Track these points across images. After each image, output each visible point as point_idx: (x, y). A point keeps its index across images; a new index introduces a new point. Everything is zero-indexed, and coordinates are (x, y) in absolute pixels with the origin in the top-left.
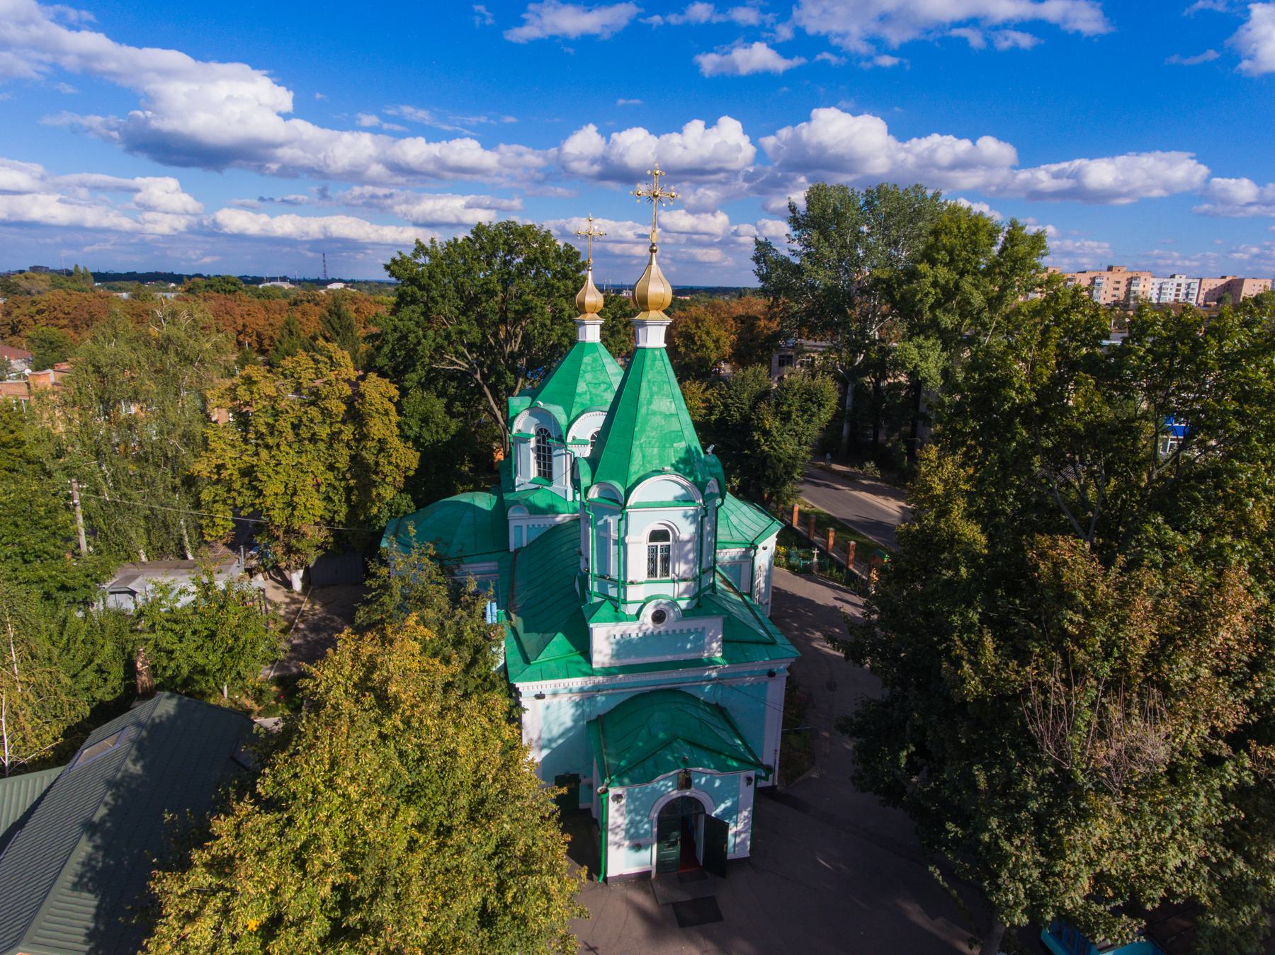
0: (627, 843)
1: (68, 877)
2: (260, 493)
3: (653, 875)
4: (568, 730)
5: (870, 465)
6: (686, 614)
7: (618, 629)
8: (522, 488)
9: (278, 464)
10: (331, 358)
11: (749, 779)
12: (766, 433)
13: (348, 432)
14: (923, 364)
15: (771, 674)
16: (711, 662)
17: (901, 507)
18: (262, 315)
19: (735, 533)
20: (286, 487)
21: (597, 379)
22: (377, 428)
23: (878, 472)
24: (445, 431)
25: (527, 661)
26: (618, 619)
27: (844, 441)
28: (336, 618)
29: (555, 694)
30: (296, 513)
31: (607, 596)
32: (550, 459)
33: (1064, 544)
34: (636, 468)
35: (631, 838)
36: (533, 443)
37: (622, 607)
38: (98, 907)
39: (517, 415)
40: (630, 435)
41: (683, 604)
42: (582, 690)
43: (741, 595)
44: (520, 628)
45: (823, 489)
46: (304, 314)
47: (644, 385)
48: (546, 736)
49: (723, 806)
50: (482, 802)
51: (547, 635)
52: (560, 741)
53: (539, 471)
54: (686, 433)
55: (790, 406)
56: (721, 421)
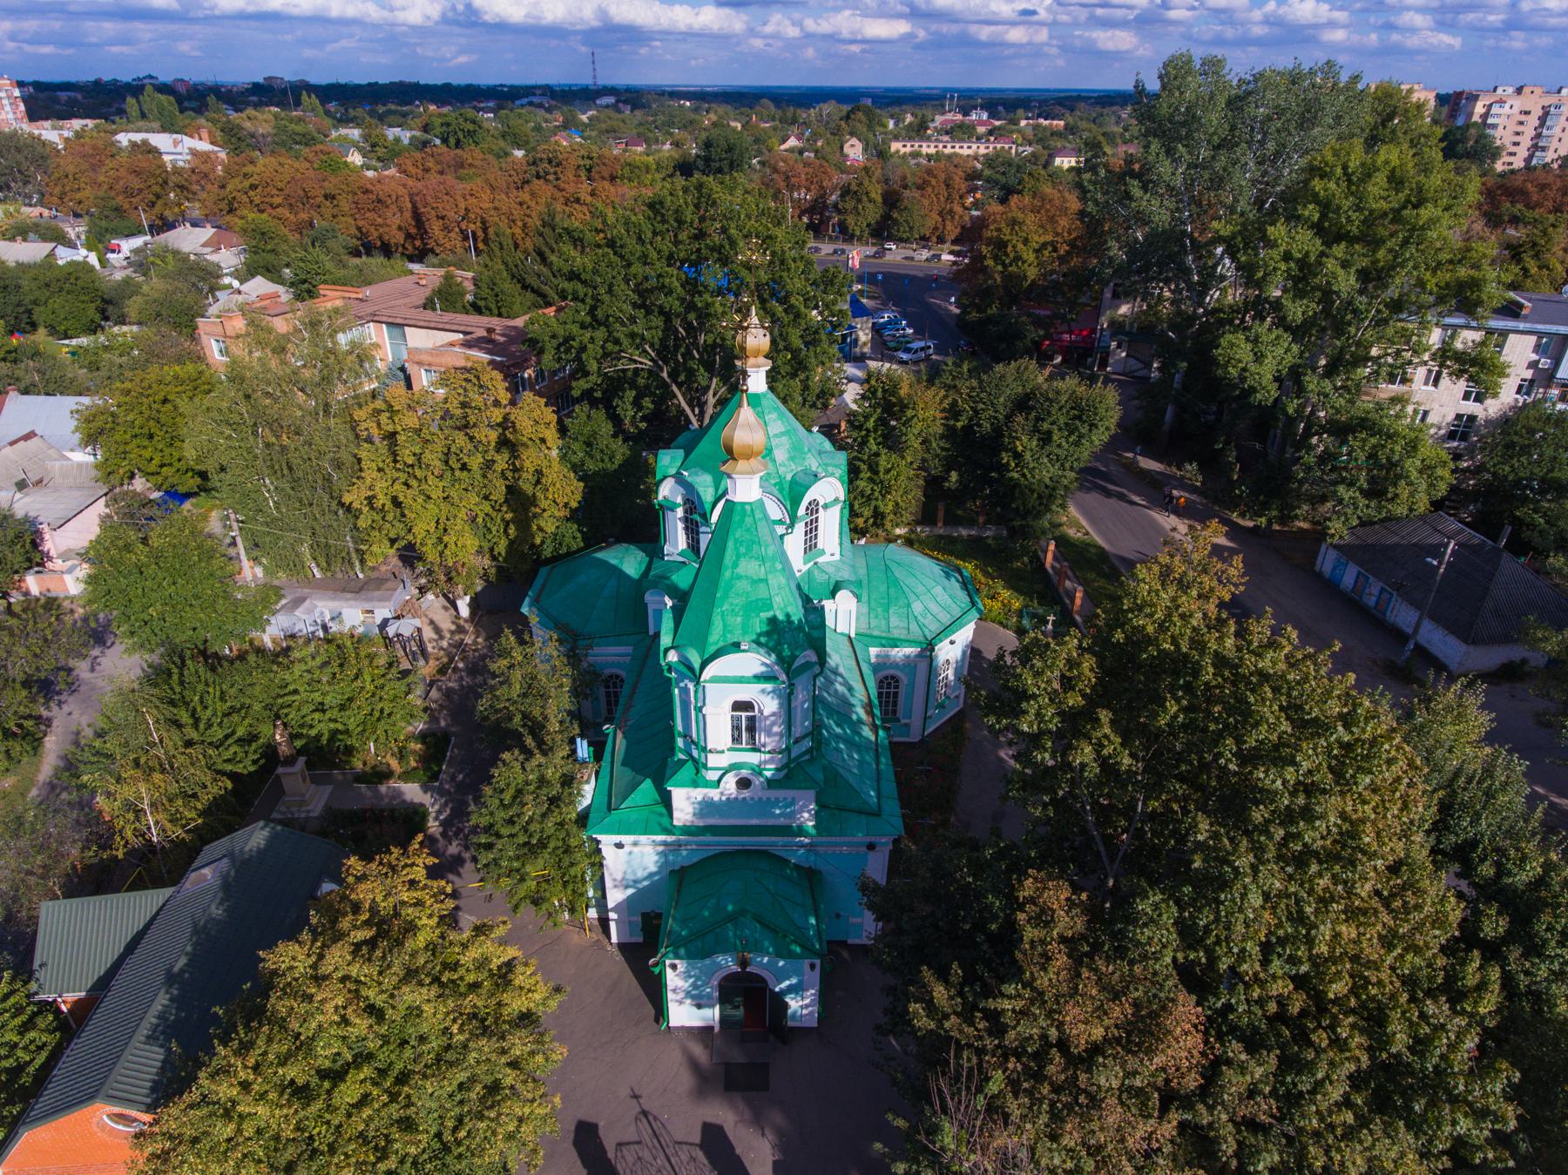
0: (688, 1001)
1: (144, 1031)
2: (410, 530)
3: (717, 1030)
4: (651, 875)
5: (1191, 468)
6: (771, 783)
7: (699, 794)
9: (429, 498)
10: (478, 378)
11: (813, 967)
12: (1018, 456)
13: (501, 461)
14: (1252, 367)
15: (871, 847)
16: (801, 831)
18: (486, 195)
19: (913, 626)
20: (437, 522)
22: (530, 460)
23: (1200, 478)
24: (611, 459)
25: (609, 809)
26: (695, 784)
27: (1166, 428)
29: (635, 844)
30: (447, 552)
31: (690, 755)
32: (698, 533)
33: (1057, 895)
34: (715, 639)
35: (693, 997)
36: (680, 512)
37: (703, 771)
38: (163, 1062)
40: (711, 600)
41: (768, 774)
42: (665, 844)
43: (875, 728)
45: (1113, 501)
46: (533, 194)
47: (730, 544)
48: (630, 877)
49: (787, 983)
50: (448, 1048)
51: (639, 777)
52: (646, 883)
54: (777, 600)
55: (1053, 423)
56: (968, 429)
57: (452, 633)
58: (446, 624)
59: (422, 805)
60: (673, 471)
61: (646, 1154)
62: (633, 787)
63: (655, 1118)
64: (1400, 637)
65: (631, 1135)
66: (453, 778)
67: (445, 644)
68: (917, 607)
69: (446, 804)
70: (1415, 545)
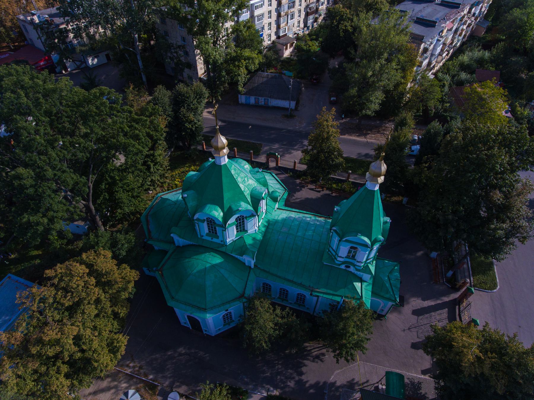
8: (232, 241)
12: (191, 122)
28: (154, 357)
39: (226, 218)
44: (331, 292)
53: (237, 232)
57: (113, 380)
58: (105, 384)
60: (222, 214)
61: (421, 331)
63: (411, 326)
64: (285, 109)
65: (415, 334)
68: (272, 185)
69: (264, 387)
70: (262, 83)
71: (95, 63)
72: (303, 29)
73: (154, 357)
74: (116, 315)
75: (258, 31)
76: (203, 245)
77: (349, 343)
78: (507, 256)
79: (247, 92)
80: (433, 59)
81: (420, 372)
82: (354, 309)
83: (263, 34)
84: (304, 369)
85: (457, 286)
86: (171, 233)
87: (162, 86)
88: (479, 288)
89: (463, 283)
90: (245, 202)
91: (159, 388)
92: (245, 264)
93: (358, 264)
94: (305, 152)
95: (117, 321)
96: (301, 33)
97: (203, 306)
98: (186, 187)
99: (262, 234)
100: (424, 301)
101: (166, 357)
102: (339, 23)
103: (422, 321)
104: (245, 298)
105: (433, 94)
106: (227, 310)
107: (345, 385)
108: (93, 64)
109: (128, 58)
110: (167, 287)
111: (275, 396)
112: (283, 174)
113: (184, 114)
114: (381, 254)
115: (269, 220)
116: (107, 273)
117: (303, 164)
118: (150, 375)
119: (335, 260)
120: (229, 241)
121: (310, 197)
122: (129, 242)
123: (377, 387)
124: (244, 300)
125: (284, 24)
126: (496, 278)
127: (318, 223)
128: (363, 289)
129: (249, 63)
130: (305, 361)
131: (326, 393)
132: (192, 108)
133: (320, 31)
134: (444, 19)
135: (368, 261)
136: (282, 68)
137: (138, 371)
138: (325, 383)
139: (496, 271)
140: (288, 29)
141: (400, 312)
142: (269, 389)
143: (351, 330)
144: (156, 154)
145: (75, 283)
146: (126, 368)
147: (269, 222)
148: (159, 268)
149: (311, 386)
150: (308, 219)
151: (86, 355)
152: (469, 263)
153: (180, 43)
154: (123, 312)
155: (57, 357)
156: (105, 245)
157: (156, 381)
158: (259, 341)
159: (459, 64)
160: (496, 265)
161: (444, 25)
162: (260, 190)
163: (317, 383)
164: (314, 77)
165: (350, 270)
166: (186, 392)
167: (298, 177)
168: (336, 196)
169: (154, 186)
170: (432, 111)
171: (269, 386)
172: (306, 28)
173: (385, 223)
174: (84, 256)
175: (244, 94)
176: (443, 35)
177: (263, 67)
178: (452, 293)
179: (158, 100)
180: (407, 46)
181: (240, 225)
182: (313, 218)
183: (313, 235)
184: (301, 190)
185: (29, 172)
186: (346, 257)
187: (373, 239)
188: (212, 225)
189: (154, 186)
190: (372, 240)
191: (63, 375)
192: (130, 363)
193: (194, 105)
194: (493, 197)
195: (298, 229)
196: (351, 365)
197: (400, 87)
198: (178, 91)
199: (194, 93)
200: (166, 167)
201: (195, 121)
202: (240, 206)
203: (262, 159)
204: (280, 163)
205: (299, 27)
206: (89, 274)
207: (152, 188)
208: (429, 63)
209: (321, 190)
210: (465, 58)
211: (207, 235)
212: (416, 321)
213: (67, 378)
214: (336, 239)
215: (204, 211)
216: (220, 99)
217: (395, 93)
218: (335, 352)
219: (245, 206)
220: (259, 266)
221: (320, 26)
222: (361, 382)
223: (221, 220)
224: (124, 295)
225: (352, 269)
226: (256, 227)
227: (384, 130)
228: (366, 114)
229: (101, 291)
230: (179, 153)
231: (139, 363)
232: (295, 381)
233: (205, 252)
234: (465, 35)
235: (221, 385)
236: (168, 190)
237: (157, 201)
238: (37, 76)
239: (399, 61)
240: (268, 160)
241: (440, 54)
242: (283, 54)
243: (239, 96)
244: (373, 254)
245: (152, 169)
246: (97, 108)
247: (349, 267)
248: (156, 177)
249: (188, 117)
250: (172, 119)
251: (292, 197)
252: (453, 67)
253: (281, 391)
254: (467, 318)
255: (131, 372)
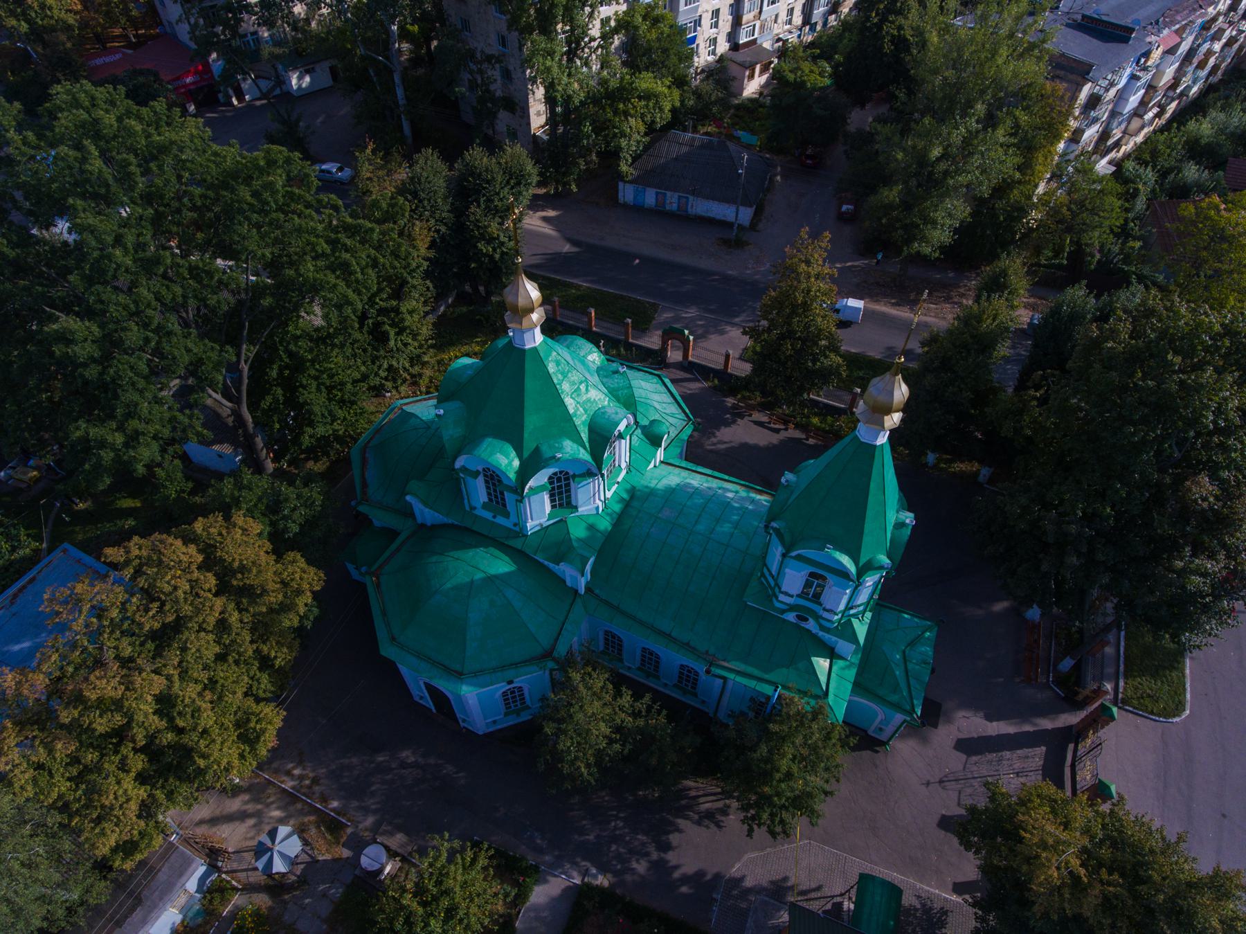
12: (491, 240)
17: (545, 219)
21: (573, 383)
28: (346, 761)
39: (526, 472)
44: (756, 672)
53: (553, 507)
55: (501, 200)
57: (256, 800)
58: (235, 805)
59: (567, 890)
60: (516, 463)
61: (969, 791)
62: (812, 671)
63: (946, 776)
65: (954, 795)
66: (539, 850)
67: (277, 813)
69: (575, 864)
70: (676, 159)
71: (304, 85)
72: (801, 30)
73: (346, 761)
74: (265, 663)
75: (682, 30)
76: (474, 528)
77: (778, 794)
78: (1211, 640)
79: (638, 176)
80: (1115, 124)
81: (951, 887)
82: (801, 715)
83: (695, 37)
84: (674, 838)
85: (1080, 697)
86: (408, 494)
87: (433, 150)
88: (1134, 708)
89: (1094, 691)
90: (573, 441)
91: (349, 831)
92: (564, 582)
93: (826, 615)
94: (752, 333)
95: (269, 675)
96: (793, 39)
97: (458, 668)
98: (446, 392)
99: (612, 519)
100: (991, 721)
101: (373, 765)
102: (884, 20)
103: (976, 768)
104: (554, 659)
105: (1102, 214)
106: (510, 682)
107: (764, 889)
108: (300, 87)
109: (375, 79)
110: (384, 614)
111: (600, 889)
112: (696, 380)
113: (477, 221)
114: (888, 597)
115: (633, 488)
116: (243, 569)
117: (746, 361)
118: (333, 799)
119: (774, 600)
120: (531, 525)
121: (752, 440)
122: (308, 504)
123: (841, 904)
124: (551, 665)
125: (752, 14)
126: (1185, 690)
127: (750, 507)
128: (833, 674)
129: (647, 106)
130: (679, 821)
131: (716, 900)
132: (496, 206)
133: (840, 37)
134: (1157, 22)
135: (852, 612)
136: (734, 125)
137: (310, 787)
138: (718, 876)
139: (1187, 671)
140: (762, 27)
141: (925, 740)
142: (587, 870)
143: (784, 764)
144: (403, 309)
145: (168, 583)
146: (285, 778)
147: (633, 492)
148: (374, 568)
149: (685, 879)
150: (730, 495)
151: (185, 739)
152: (1122, 644)
153: (494, 49)
154: (281, 657)
155: (120, 735)
156: (256, 505)
157: (344, 815)
158: (572, 762)
159: (1186, 142)
160: (1191, 658)
161: (1153, 38)
162: (613, 416)
163: (700, 874)
164: (809, 152)
165: (807, 627)
166: (402, 846)
167: (732, 392)
168: (815, 446)
169: (395, 380)
170: (1093, 256)
171: (588, 864)
172: (808, 28)
173: (899, 525)
174: (199, 525)
175: (630, 182)
176: (1149, 63)
177: (678, 119)
178: (1063, 712)
179: (420, 183)
180: (1043, 87)
181: (560, 493)
182: (743, 493)
183: (732, 535)
184: (734, 422)
185: (88, 328)
186: (798, 596)
187: (863, 560)
188: (494, 485)
189: (395, 380)
190: (861, 564)
191: (133, 774)
192: (294, 768)
193: (501, 200)
194: (1190, 490)
195: (700, 516)
196: (786, 846)
197: (1015, 192)
198: (468, 164)
199: (504, 173)
200: (426, 341)
201: (502, 239)
202: (560, 449)
203: (653, 341)
204: (693, 355)
205: (790, 22)
206: (205, 566)
207: (389, 384)
208: (1105, 135)
209: (783, 427)
210: (1204, 128)
211: (485, 506)
212: (961, 767)
213: (142, 783)
214: (777, 550)
215: (476, 453)
216: (575, 190)
217: (999, 204)
218: (748, 812)
219: (573, 451)
220: (597, 591)
221: (845, 25)
222: (802, 888)
223: (512, 476)
224: (290, 621)
225: (811, 625)
226: (597, 501)
227: (962, 295)
228: (919, 252)
229: (231, 606)
230: (464, 309)
231: (313, 771)
232: (650, 862)
233: (476, 547)
234: (1215, 68)
235: (476, 845)
236: (428, 393)
237: (391, 416)
238: (138, 110)
239: (1017, 126)
240: (664, 343)
241: (1138, 113)
242: (742, 89)
243: (621, 185)
244: (863, 597)
245: (392, 343)
246: (255, 194)
247: (806, 620)
248: (402, 362)
249: (486, 227)
250: (449, 228)
251: (709, 438)
252: (1169, 147)
253: (615, 879)
254: (1088, 778)
255: (293, 788)
